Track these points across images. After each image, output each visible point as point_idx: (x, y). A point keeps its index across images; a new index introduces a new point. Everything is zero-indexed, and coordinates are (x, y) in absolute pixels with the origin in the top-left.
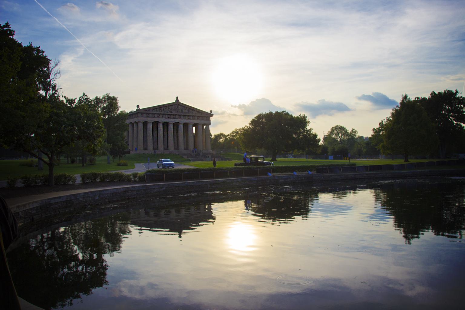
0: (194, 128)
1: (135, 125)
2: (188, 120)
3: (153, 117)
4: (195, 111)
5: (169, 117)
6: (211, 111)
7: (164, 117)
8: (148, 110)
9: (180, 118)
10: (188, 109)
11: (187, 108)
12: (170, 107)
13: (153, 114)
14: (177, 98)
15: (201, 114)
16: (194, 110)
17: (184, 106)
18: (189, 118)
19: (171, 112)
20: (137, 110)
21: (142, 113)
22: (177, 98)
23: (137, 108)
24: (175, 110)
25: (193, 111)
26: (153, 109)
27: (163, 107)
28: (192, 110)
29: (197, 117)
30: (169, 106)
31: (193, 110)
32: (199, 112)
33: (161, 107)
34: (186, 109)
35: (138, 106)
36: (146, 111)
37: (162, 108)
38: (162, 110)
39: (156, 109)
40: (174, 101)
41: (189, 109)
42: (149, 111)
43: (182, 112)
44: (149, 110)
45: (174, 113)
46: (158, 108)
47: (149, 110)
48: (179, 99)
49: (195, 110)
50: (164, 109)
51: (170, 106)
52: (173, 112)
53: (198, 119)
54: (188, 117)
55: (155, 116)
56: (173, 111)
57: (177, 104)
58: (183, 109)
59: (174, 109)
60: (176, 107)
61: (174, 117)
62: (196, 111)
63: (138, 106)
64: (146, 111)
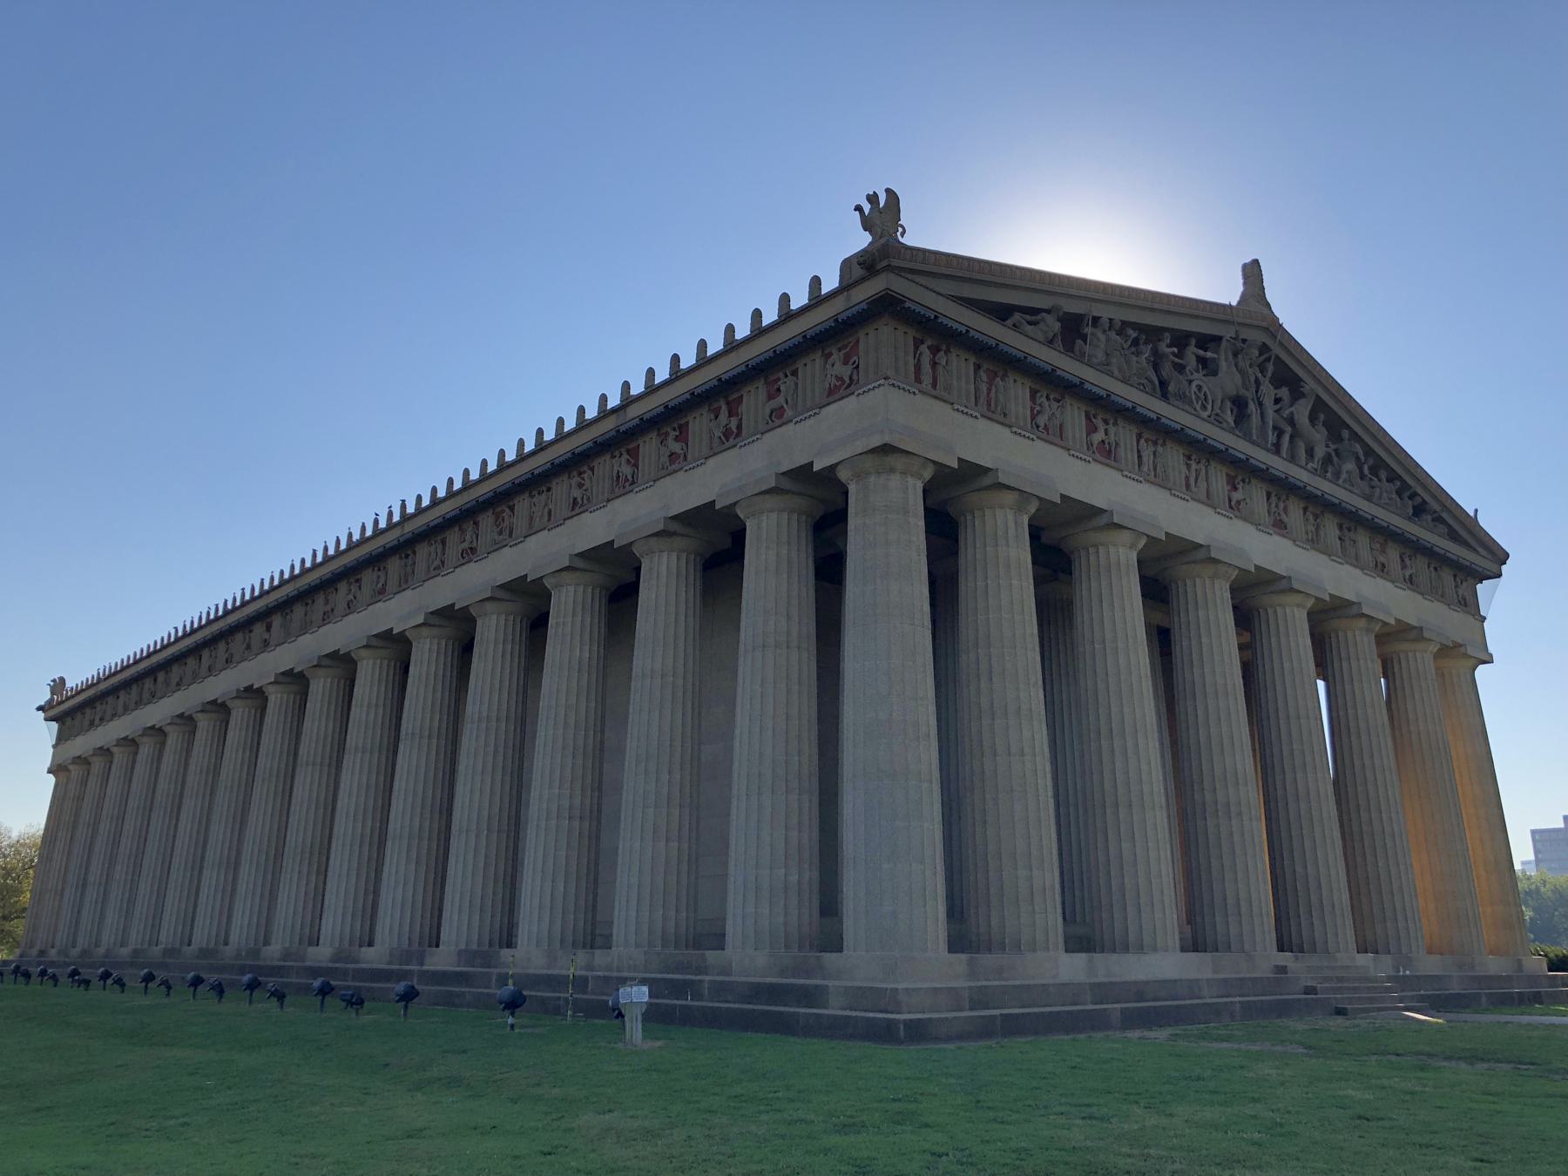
20: (862, 267)
23: (861, 240)
61: (1238, 502)
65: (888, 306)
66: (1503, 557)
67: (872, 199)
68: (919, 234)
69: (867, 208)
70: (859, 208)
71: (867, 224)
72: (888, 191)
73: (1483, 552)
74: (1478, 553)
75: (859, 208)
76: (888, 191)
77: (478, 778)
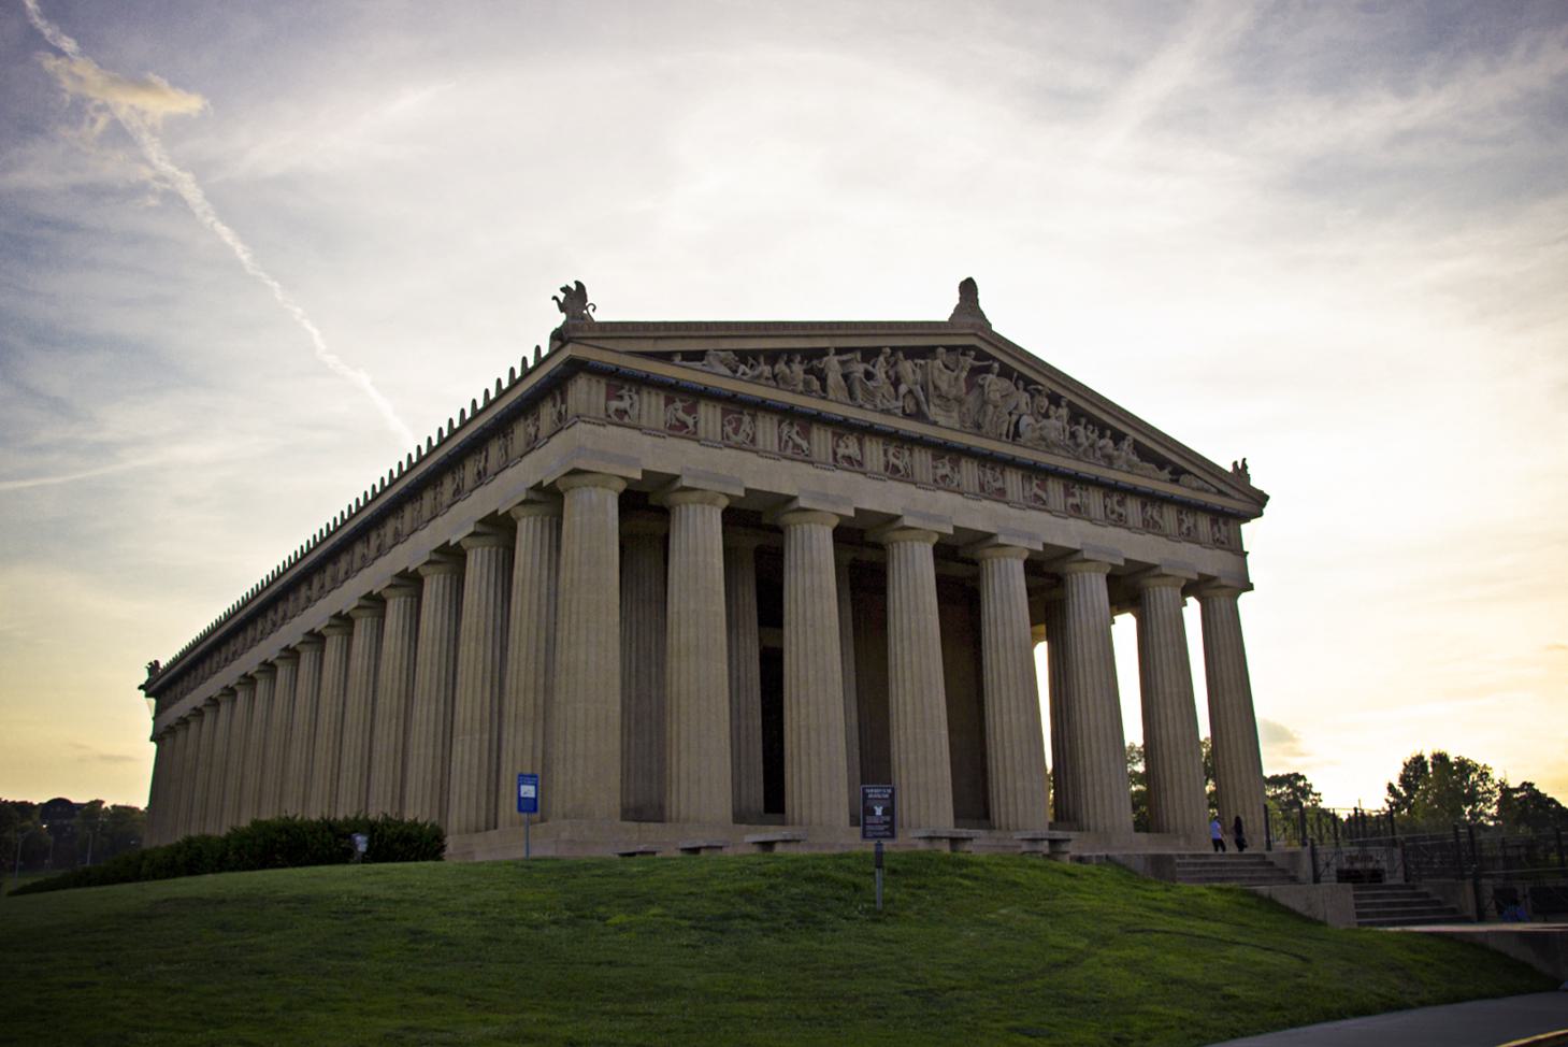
0: (1041, 652)
1: (528, 534)
2: (1071, 521)
3: (738, 447)
4: (1125, 445)
5: (896, 469)
6: (1241, 471)
7: (849, 459)
8: (690, 356)
9: (1002, 492)
10: (1064, 412)
11: (1055, 400)
12: (906, 367)
13: (733, 404)
14: (968, 288)
15: (1175, 481)
16: (1118, 437)
17: (1028, 382)
18: (1077, 508)
19: (919, 415)
20: (558, 336)
21: (617, 379)
22: (968, 288)
23: (559, 319)
24: (960, 401)
25: (1107, 442)
26: (743, 356)
27: (839, 351)
28: (1101, 436)
29: (1144, 506)
30: (894, 350)
31: (1103, 428)
32: (1161, 463)
33: (823, 352)
34: (1046, 416)
35: (574, 299)
36: (666, 357)
37: (832, 364)
38: (834, 377)
39: (773, 356)
40: (940, 307)
41: (1076, 415)
42: (697, 365)
43: (1017, 434)
44: (699, 356)
45: (945, 425)
46: (790, 354)
47: (699, 356)
48: (985, 303)
49: (1123, 436)
50: (846, 377)
51: (912, 353)
52: (942, 420)
53: (1150, 526)
54: (1068, 494)
55: (760, 437)
56: (934, 412)
57: (965, 350)
58: (1023, 407)
59: (944, 386)
60: (964, 374)
61: (944, 477)
62: (1138, 448)
63: (574, 299)
64: (666, 357)
65: (575, 367)
66: (1267, 498)
67: (565, 290)
68: (604, 309)
69: (561, 296)
70: (555, 298)
71: (562, 308)
72: (577, 283)
73: (1237, 495)
74: (1233, 498)
75: (555, 298)
76: (577, 283)
77: (394, 721)
